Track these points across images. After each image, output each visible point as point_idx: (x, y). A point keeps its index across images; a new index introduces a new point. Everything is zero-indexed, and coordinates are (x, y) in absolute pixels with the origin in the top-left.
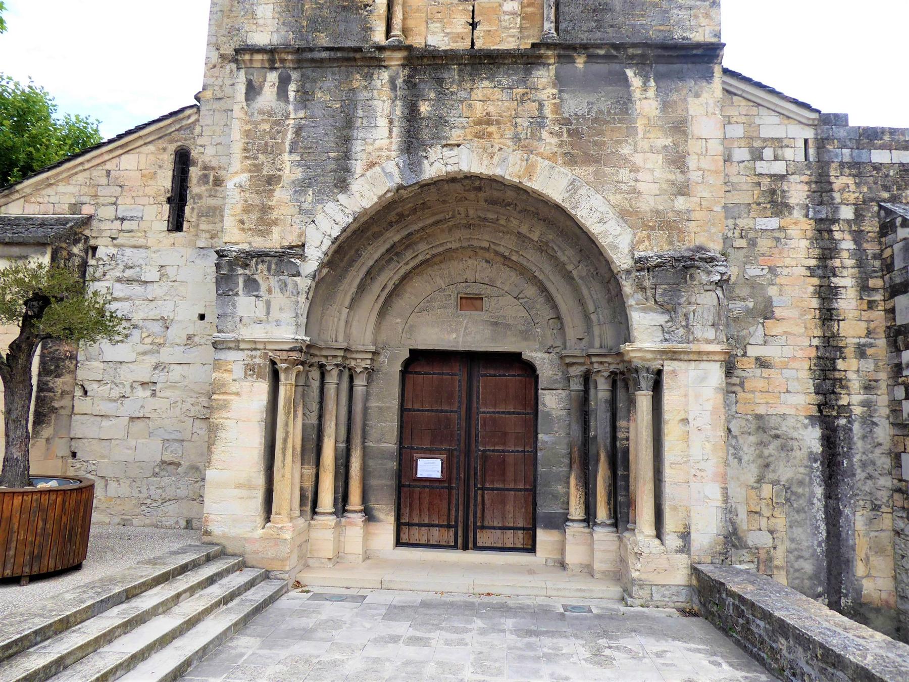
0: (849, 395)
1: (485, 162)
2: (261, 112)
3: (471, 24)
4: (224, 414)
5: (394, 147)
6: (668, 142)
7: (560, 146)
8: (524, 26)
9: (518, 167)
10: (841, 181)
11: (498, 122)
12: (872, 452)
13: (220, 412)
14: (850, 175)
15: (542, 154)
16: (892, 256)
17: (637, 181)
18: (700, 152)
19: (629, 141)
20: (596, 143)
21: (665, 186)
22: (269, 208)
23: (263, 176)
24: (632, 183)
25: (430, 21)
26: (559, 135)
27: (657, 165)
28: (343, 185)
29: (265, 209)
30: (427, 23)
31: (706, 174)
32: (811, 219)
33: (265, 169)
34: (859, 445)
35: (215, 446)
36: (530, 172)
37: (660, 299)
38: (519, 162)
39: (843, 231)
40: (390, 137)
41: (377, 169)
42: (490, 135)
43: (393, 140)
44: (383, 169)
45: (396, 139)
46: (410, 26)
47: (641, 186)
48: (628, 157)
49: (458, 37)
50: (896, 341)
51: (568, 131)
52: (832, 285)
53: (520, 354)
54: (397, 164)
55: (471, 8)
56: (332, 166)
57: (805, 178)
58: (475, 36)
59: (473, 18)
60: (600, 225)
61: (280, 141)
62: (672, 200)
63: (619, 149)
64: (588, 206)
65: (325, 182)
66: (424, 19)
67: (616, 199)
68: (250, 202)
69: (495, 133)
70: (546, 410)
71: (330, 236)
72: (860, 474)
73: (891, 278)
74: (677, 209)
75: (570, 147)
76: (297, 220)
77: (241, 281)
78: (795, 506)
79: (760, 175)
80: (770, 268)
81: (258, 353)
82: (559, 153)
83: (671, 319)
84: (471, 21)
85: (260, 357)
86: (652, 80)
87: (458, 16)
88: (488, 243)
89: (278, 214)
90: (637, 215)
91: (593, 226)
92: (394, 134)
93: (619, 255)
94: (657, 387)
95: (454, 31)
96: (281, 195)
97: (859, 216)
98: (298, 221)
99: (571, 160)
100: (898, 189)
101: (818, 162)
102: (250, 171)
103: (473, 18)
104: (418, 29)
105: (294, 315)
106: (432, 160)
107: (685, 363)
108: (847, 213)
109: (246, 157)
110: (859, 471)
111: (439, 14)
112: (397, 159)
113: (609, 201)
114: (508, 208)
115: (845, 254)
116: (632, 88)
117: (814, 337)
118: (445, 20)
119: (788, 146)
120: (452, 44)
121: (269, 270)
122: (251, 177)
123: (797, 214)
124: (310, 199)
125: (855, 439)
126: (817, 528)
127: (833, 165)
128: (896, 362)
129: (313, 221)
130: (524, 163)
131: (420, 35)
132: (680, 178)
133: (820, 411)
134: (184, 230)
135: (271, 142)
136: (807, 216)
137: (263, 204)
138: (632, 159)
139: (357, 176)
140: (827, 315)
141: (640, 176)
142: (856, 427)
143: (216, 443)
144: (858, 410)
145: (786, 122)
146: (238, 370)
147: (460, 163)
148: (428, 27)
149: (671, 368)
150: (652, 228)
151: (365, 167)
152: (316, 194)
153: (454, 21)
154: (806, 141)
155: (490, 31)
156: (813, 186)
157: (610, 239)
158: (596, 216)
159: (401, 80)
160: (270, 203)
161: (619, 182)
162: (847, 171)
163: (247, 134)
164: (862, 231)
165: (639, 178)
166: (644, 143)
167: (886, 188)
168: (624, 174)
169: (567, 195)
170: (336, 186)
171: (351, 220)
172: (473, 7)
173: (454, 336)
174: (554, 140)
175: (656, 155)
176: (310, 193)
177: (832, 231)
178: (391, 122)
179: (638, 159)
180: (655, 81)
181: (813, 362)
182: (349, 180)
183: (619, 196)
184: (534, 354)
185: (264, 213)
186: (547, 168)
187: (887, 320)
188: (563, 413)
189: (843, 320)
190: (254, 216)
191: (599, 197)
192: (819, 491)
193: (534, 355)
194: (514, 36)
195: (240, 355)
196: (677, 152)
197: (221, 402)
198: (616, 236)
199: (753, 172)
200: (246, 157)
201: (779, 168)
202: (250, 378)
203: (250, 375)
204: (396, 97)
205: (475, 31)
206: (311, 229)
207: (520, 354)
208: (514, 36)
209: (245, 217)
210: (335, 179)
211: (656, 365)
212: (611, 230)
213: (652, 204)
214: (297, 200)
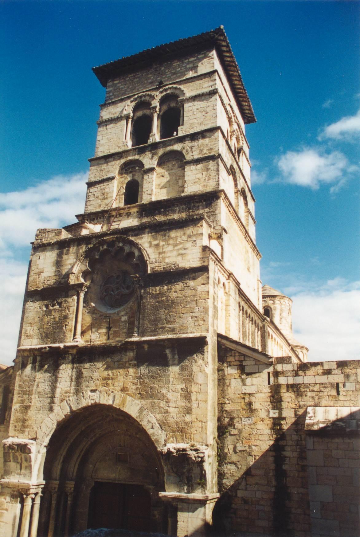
1: (106, 398)
2: (26, 376)
5: (72, 391)
6: (183, 386)
7: (137, 389)
8: (129, 327)
11: (112, 379)
15: (129, 394)
18: (197, 391)
19: (166, 386)
20: (152, 388)
21: (181, 409)
23: (24, 405)
24: (167, 408)
26: (136, 384)
28: (51, 409)
29: (24, 421)
31: (200, 402)
33: (26, 402)
36: (123, 402)
38: (119, 398)
40: (71, 387)
42: (108, 384)
43: (71, 388)
45: (73, 388)
47: (170, 410)
48: (165, 394)
51: (140, 382)
52: (282, 456)
55: (109, 320)
56: (49, 400)
59: (109, 325)
61: (31, 389)
62: (184, 417)
64: (147, 420)
67: (159, 416)
68: (19, 417)
69: (110, 384)
74: (186, 421)
75: (141, 390)
77: (11, 455)
79: (245, 394)
80: (249, 446)
86: (177, 355)
90: (168, 424)
91: (149, 430)
92: (72, 385)
93: (159, 445)
96: (31, 413)
99: (142, 397)
102: (20, 403)
103: (109, 325)
106: (85, 397)
109: (19, 397)
116: (169, 359)
122: (21, 406)
132: (188, 405)
134: (5, 424)
135: (28, 389)
136: (268, 415)
138: (167, 395)
141: (171, 404)
158: (150, 425)
159: (76, 359)
160: (26, 418)
162: (290, 389)
163: (20, 386)
165: (169, 405)
166: (173, 387)
168: (163, 404)
169: (138, 414)
174: (134, 387)
175: (177, 393)
177: (282, 424)
178: (71, 379)
179: (170, 396)
180: (178, 355)
182: (54, 408)
183: (160, 415)
186: (131, 401)
190: (20, 424)
191: (152, 415)
194: (125, 333)
196: (187, 391)
199: (241, 393)
200: (19, 397)
204: (74, 367)
206: (39, 431)
208: (125, 333)
209: (17, 424)
212: (156, 433)
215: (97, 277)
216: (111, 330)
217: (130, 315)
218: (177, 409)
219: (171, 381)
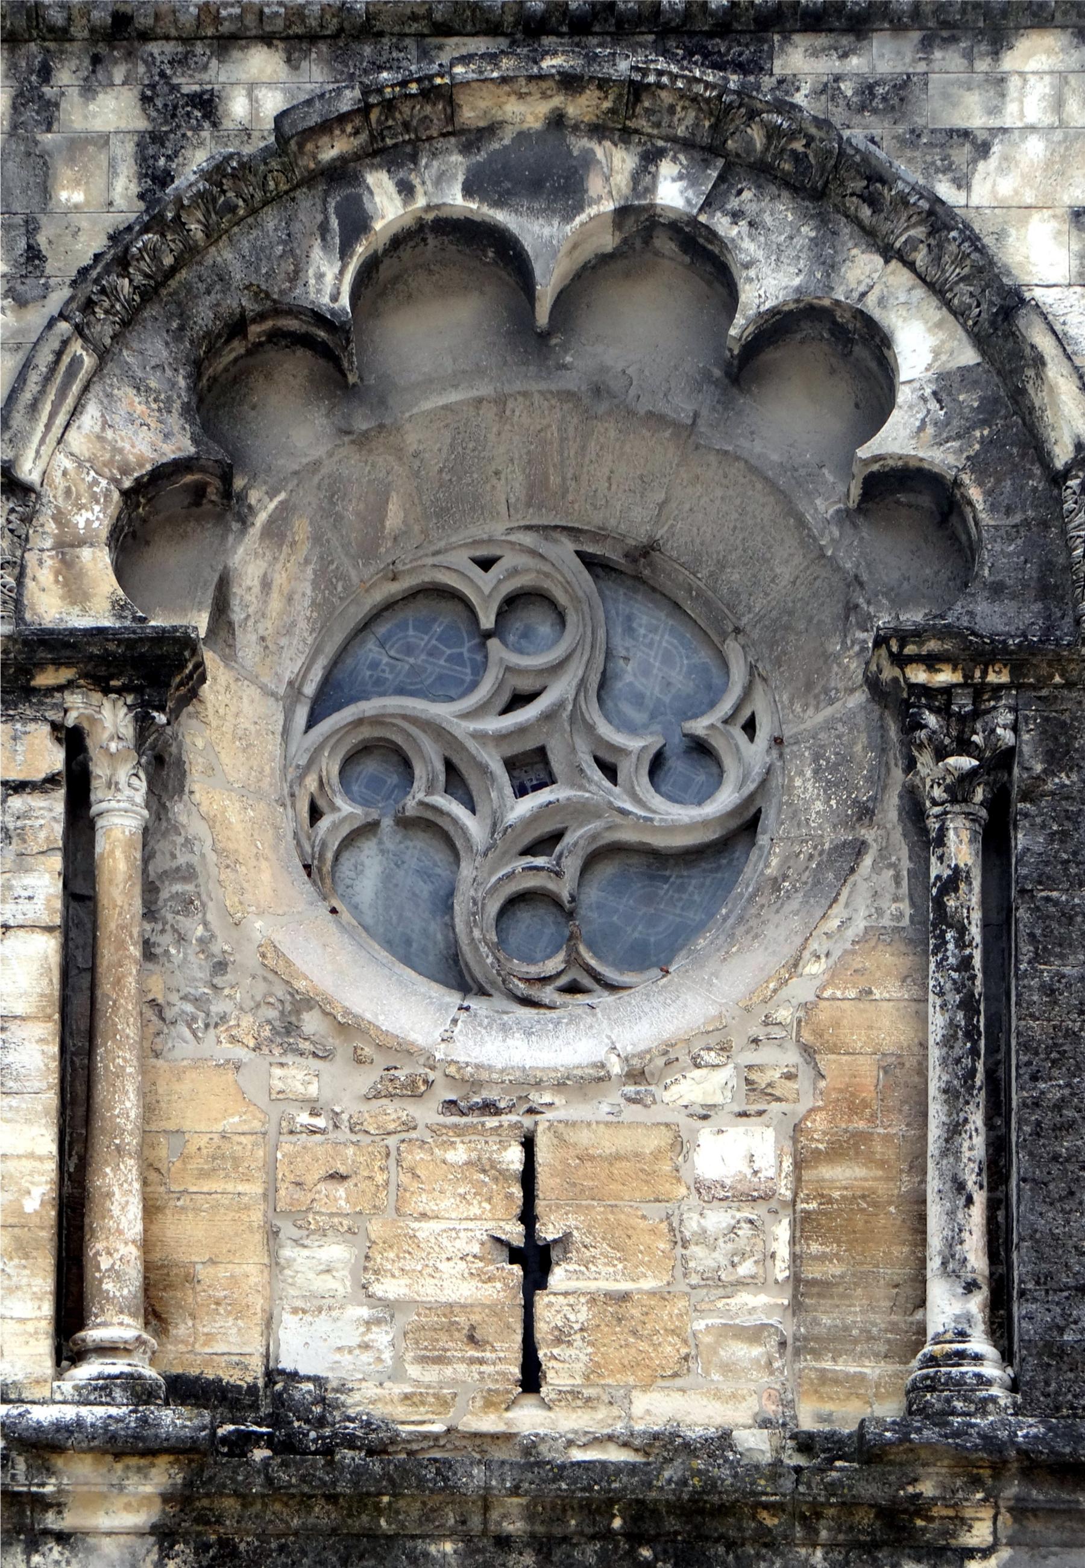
3: (515, 1255)
25: (288, 1230)
30: (273, 1234)
46: (181, 1255)
49: (451, 1328)
55: (514, 1157)
58: (542, 1329)
59: (528, 1217)
66: (256, 1217)
84: (515, 1232)
87: (446, 1204)
95: (428, 1291)
103: (528, 1217)
104: (222, 1272)
111: (340, 1191)
118: (375, 1228)
120: (414, 1371)
131: (240, 1311)
148: (275, 1265)
153: (425, 1230)
155: (624, 1297)
172: (529, 1144)
205: (541, 1300)
215: (266, 585)
216: (558, 1277)
217: (819, 1123)
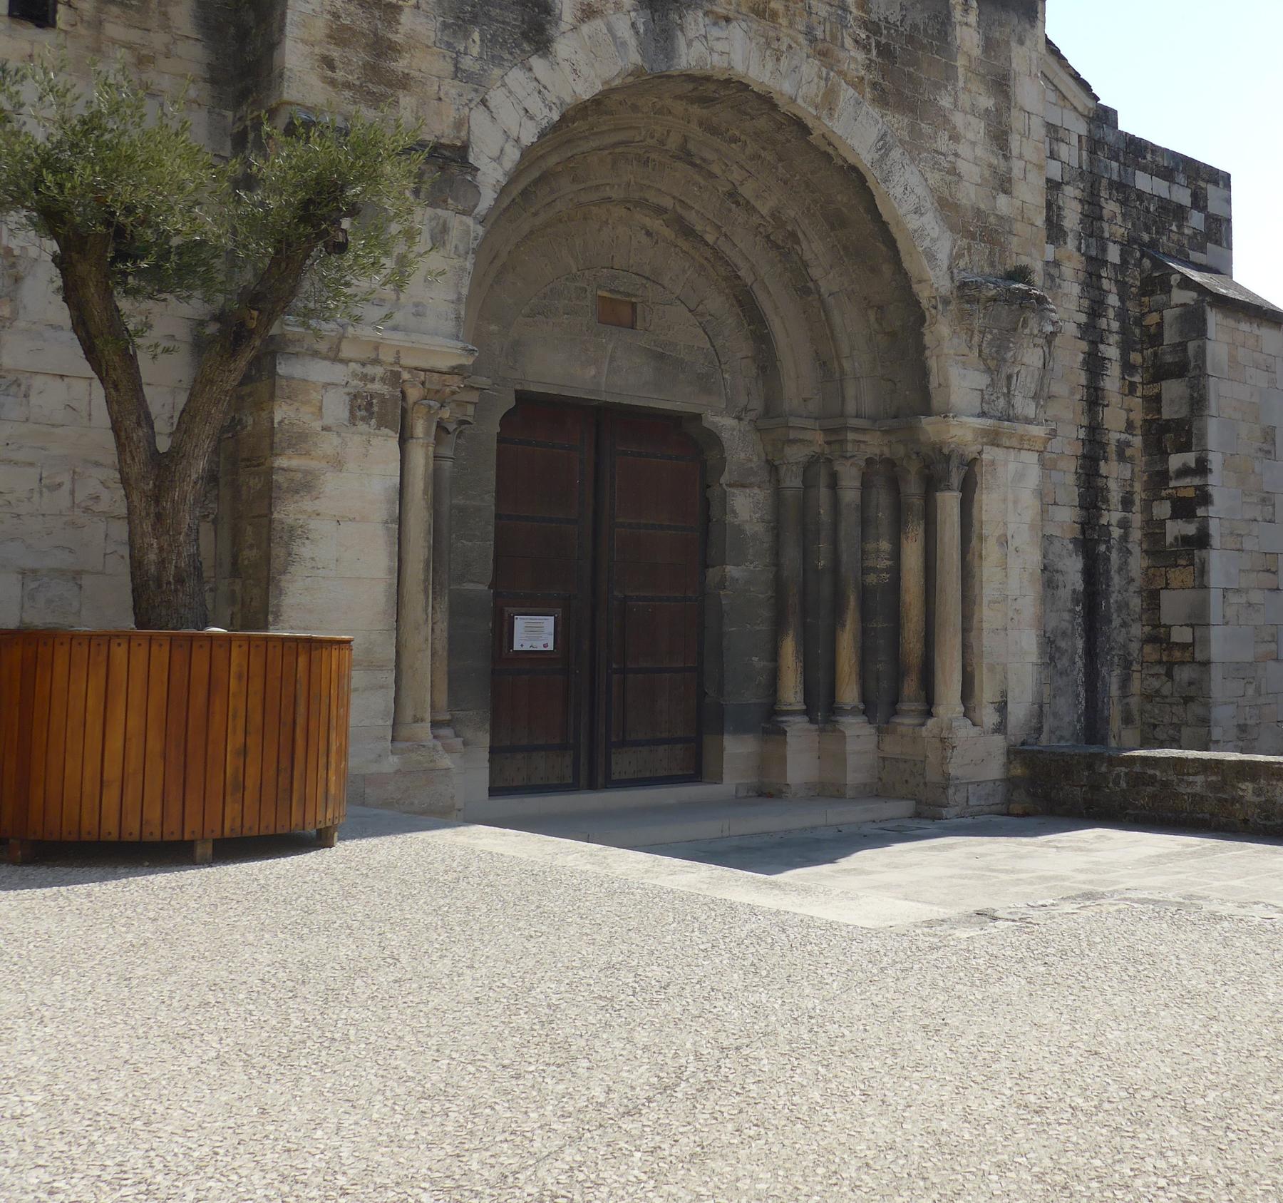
0: (1109, 511)
4: (307, 505)
9: (814, 85)
10: (1111, 207)
12: (1126, 591)
13: (297, 497)
14: (1118, 201)
16: (1160, 325)
17: (956, 155)
21: (987, 174)
22: (389, 48)
24: (951, 158)
27: (979, 136)
32: (1083, 255)
34: (1116, 580)
35: (288, 577)
37: (986, 351)
39: (1110, 279)
41: (598, 24)
44: (610, 30)
50: (1159, 441)
53: (698, 417)
54: (633, 25)
57: (1078, 193)
60: (916, 217)
63: (938, 97)
65: (503, 23)
67: (935, 178)
70: (737, 522)
71: (517, 140)
72: (1116, 622)
73: (1155, 354)
76: (451, 89)
78: (1059, 666)
81: (378, 371)
82: (866, 78)
83: (993, 384)
85: (383, 379)
88: (672, 201)
89: (410, 67)
94: (968, 489)
97: (1124, 261)
98: (453, 92)
100: (1157, 233)
101: (1091, 172)
105: (454, 297)
107: (1005, 450)
108: (1114, 254)
110: (1115, 616)
112: (633, 14)
113: (926, 180)
114: (733, 145)
115: (1111, 313)
117: (1082, 427)
119: (1063, 141)
121: (416, 192)
123: (1071, 243)
124: (475, 50)
125: (1112, 573)
126: (1078, 695)
127: (1104, 182)
128: (1158, 468)
129: (484, 102)
130: (823, 83)
133: (1083, 533)
136: (1079, 250)
137: (376, 35)
139: (564, 26)
140: (1094, 399)
141: (963, 149)
142: (1114, 556)
143: (291, 569)
144: (1116, 532)
145: (1062, 103)
146: (336, 407)
147: (732, 55)
149: (991, 458)
150: (972, 236)
151: (579, 14)
152: (490, 41)
154: (1080, 136)
156: (1086, 207)
157: (927, 243)
160: (397, 39)
161: (936, 151)
164: (1126, 283)
165: (959, 152)
167: (1148, 230)
170: (525, 35)
171: (556, 117)
173: (592, 371)
176: (476, 36)
177: (1100, 277)
179: (958, 119)
181: (1080, 461)
182: (552, 31)
183: (938, 175)
184: (716, 419)
185: (378, 56)
187: (1147, 410)
188: (759, 528)
189: (1107, 406)
192: (1080, 644)
193: (724, 423)
195: (338, 373)
197: (300, 475)
198: (934, 241)
201: (1055, 170)
202: (362, 427)
203: (363, 419)
206: (479, 118)
207: (698, 417)
210: (523, 22)
211: (972, 450)
213: (973, 196)
214: (449, 45)
218: (978, 169)
219: (961, 71)
